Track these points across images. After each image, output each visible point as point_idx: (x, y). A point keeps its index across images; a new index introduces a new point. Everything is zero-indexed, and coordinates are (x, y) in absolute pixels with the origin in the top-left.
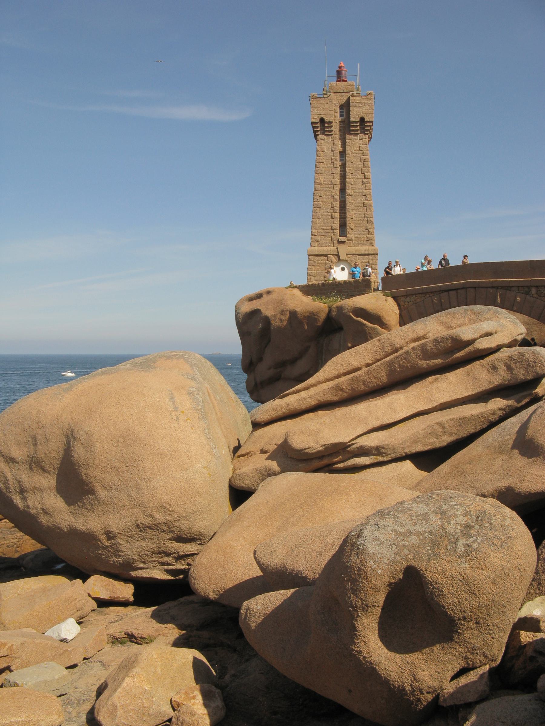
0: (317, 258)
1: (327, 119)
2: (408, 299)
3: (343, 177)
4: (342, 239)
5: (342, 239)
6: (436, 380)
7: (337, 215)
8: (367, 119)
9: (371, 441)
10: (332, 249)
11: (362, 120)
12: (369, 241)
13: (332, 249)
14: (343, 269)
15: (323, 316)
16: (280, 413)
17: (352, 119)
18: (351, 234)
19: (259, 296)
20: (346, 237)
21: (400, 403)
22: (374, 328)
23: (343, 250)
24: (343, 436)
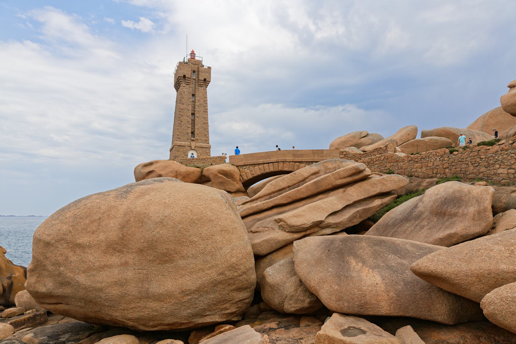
2: (245, 167)
3: (194, 107)
6: (344, 191)
7: (190, 126)
8: (207, 80)
9: (332, 220)
11: (205, 80)
12: (207, 141)
15: (198, 175)
16: (251, 211)
17: (200, 79)
18: (197, 137)
19: (151, 164)
20: (194, 137)
21: (333, 201)
22: (229, 181)
23: (193, 144)
24: (320, 217)
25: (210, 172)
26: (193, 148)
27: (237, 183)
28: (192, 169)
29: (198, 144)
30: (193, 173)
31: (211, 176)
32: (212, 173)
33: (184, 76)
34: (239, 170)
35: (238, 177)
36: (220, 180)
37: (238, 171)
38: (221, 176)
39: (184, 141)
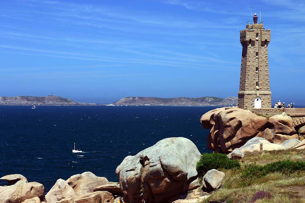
0: (248, 96)
1: (252, 40)
4: (257, 87)
5: (257, 87)
10: (254, 92)
13: (254, 92)
14: (258, 100)
15: (265, 122)
23: (258, 93)
25: (273, 121)
26: (258, 96)
27: (291, 128)
28: (261, 118)
29: (262, 92)
30: (262, 121)
31: (274, 123)
32: (275, 122)
33: (250, 40)
34: (293, 119)
35: (291, 124)
36: (280, 126)
37: (292, 120)
38: (280, 123)
39: (251, 90)
